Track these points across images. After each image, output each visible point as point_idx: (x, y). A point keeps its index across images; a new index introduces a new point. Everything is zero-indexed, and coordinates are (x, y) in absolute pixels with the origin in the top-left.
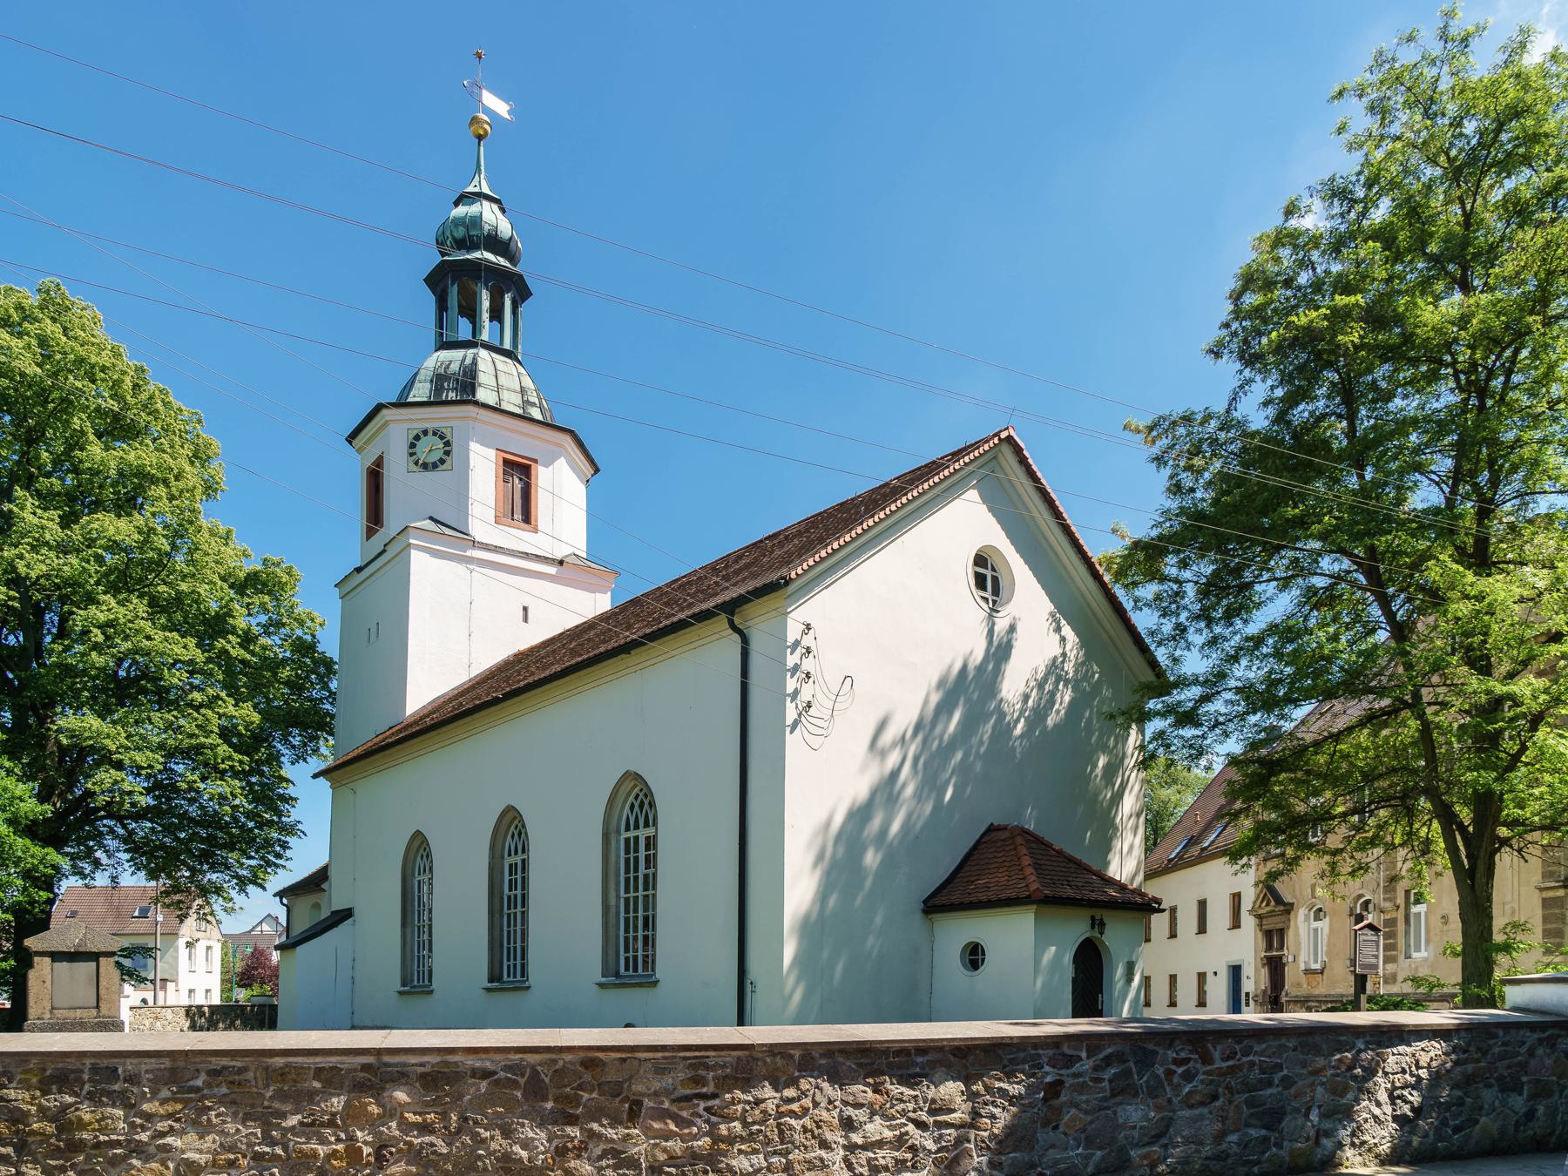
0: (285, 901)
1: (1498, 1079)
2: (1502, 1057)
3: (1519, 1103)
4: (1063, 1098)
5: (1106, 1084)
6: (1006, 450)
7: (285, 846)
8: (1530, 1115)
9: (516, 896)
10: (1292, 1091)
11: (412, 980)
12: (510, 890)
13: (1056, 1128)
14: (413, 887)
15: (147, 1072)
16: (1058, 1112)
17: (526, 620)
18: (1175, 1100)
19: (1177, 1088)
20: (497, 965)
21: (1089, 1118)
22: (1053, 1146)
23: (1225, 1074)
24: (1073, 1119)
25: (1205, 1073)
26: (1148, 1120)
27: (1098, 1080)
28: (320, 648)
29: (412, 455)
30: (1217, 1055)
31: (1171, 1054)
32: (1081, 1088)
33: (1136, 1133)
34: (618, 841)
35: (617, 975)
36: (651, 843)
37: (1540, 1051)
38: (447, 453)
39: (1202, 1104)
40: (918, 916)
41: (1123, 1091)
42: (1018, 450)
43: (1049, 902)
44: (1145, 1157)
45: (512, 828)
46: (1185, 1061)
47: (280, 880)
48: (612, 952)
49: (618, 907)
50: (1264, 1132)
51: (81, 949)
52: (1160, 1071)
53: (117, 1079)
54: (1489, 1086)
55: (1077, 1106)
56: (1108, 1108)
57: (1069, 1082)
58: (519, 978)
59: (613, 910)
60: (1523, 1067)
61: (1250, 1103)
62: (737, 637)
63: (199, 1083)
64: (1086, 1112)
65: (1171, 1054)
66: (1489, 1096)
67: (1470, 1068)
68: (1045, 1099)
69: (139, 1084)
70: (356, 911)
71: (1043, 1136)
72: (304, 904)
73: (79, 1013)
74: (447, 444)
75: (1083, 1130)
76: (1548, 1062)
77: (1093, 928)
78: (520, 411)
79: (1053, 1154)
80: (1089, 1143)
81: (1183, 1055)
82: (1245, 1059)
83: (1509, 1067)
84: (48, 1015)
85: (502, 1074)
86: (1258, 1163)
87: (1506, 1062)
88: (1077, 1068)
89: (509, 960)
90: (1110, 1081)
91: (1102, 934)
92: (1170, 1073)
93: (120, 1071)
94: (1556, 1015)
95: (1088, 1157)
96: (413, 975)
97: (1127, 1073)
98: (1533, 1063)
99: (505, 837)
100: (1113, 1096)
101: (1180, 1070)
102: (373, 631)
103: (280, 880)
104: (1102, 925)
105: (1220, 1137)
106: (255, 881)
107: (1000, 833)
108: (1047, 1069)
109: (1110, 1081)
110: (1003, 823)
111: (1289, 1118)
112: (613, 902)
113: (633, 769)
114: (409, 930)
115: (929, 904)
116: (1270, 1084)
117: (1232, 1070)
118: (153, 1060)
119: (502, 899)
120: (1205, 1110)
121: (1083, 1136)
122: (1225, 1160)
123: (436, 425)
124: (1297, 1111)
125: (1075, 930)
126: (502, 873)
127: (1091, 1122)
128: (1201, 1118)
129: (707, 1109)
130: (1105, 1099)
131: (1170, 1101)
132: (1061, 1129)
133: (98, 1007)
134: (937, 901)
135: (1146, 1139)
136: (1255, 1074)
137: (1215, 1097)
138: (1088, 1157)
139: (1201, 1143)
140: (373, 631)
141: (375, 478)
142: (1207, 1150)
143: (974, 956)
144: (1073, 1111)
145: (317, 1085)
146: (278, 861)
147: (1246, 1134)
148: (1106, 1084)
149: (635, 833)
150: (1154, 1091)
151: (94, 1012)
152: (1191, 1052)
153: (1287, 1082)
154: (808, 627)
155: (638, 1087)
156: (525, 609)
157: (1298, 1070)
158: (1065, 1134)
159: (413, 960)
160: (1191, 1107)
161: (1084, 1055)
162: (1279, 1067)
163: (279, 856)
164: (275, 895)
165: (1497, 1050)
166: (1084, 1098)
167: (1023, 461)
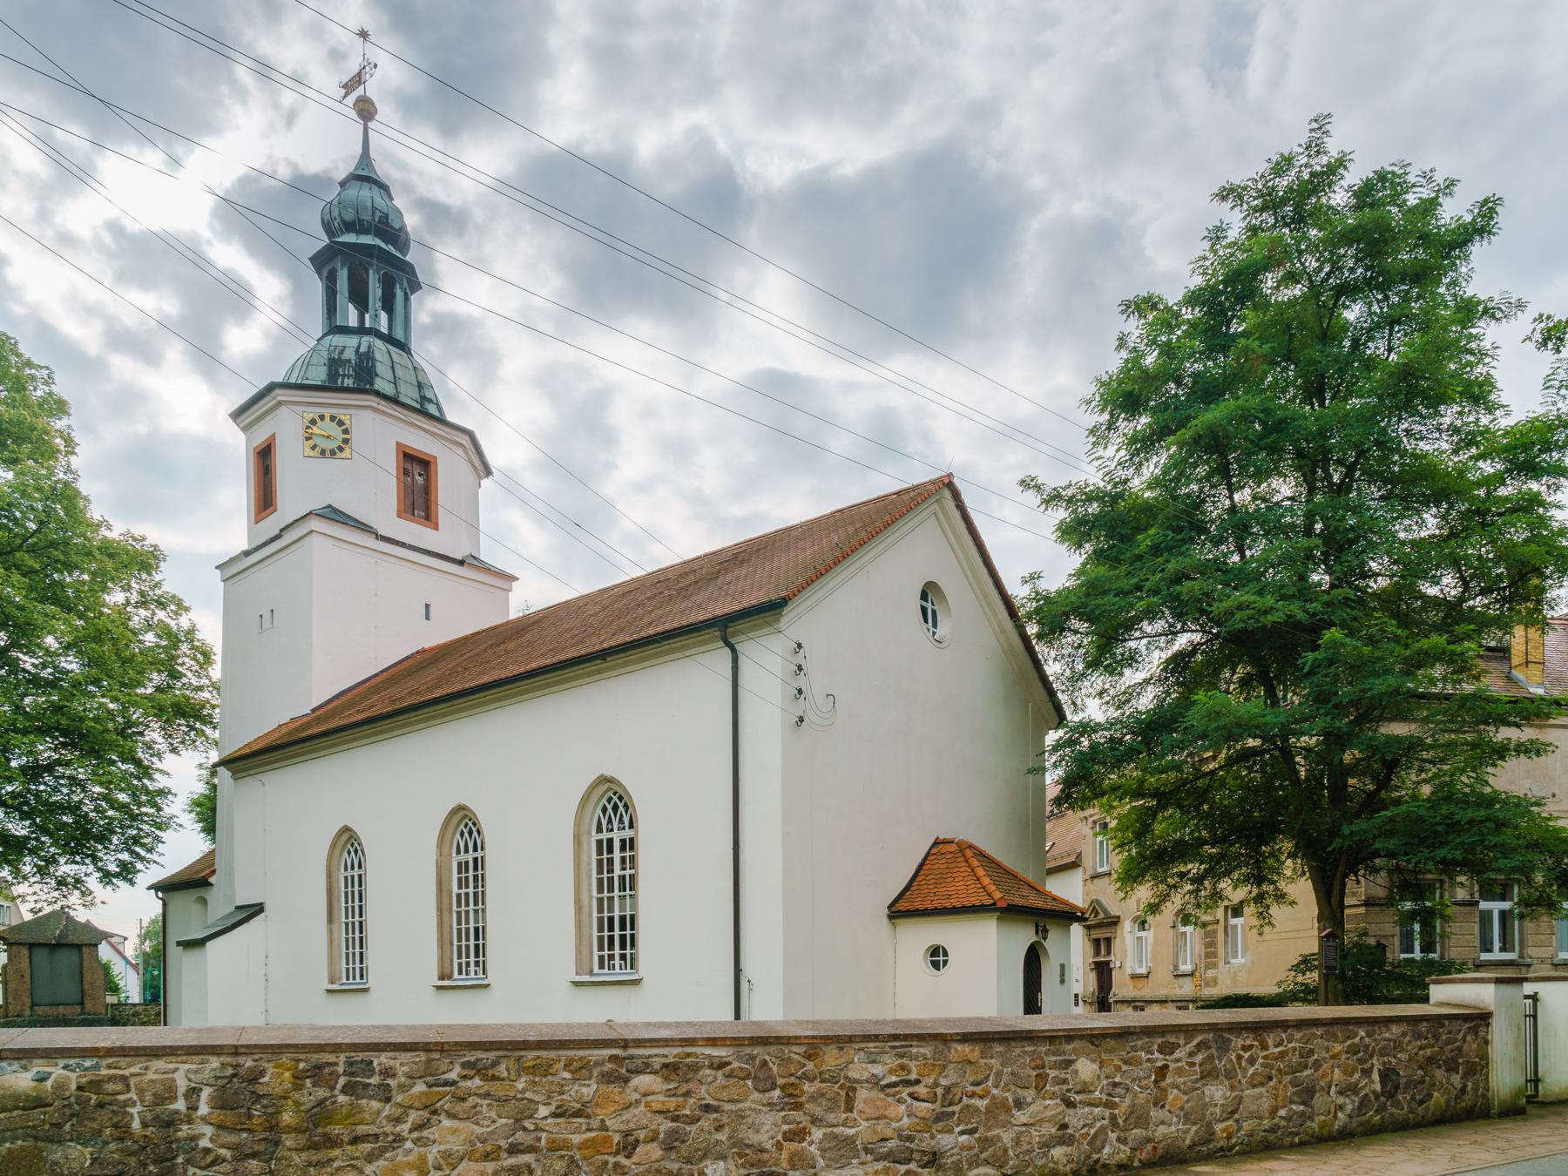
0: (160, 895)
1: (1445, 1062)
2: (1448, 1042)
3: (1456, 1079)
4: (1168, 1081)
5: (1197, 1067)
6: (947, 494)
7: (158, 839)
8: (1463, 1090)
9: (467, 895)
10: (1320, 1072)
11: (340, 978)
12: (460, 887)
13: (1163, 1106)
14: (338, 882)
15: (401, 1064)
16: (1164, 1090)
17: (427, 618)
18: (1243, 1081)
19: (1244, 1070)
20: (447, 964)
21: (1186, 1098)
22: (1162, 1123)
23: (1276, 1059)
24: (1175, 1099)
25: (1265, 1057)
26: (1226, 1098)
27: (1192, 1064)
28: (199, 636)
29: (308, 439)
30: (1270, 1042)
31: (1240, 1042)
32: (1180, 1072)
33: (1218, 1110)
34: (589, 843)
35: (591, 973)
36: (629, 845)
37: (1469, 1038)
38: (346, 441)
39: (1262, 1084)
40: (885, 920)
41: (1210, 1073)
42: (956, 496)
43: (1011, 912)
44: (1224, 1130)
45: (462, 827)
46: (1251, 1047)
47: (150, 875)
48: (585, 951)
49: (590, 906)
50: (1302, 1108)
51: (62, 941)
52: (1233, 1057)
53: (372, 1073)
54: (1439, 1067)
55: (1178, 1087)
56: (1198, 1089)
57: (1172, 1066)
58: (472, 975)
59: (585, 910)
60: (1460, 1049)
61: (1294, 1083)
62: (727, 650)
63: (453, 1075)
64: (1185, 1093)
65: (1240, 1042)
66: (1440, 1074)
67: (1429, 1052)
68: (1156, 1082)
69: (394, 1076)
70: (267, 907)
71: (1156, 1114)
72: (184, 902)
73: (61, 1009)
74: (346, 431)
75: (1182, 1109)
76: (1474, 1046)
77: (1037, 933)
78: (418, 406)
79: (1162, 1129)
80: (1187, 1118)
81: (1248, 1042)
82: (1290, 1046)
83: (1452, 1051)
84: (28, 1012)
85: (736, 1065)
86: (1298, 1134)
87: (1449, 1047)
88: (1177, 1054)
89: (460, 957)
90: (1200, 1065)
91: (1045, 939)
92: (1239, 1058)
93: (375, 1064)
94: (1475, 1008)
95: (1186, 1132)
96: (340, 972)
97: (1210, 1058)
98: (1465, 1047)
99: (454, 833)
100: (1202, 1078)
101: (1247, 1055)
102: (267, 617)
103: (150, 875)
104: (1045, 931)
105: (1273, 1112)
106: (127, 872)
107: (947, 846)
108: (1157, 1055)
109: (1200, 1065)
110: (949, 836)
111: (1317, 1095)
112: (585, 901)
113: (608, 773)
114: (335, 926)
115: (893, 909)
116: (1306, 1067)
117: (1282, 1055)
118: (409, 1054)
119: (451, 896)
120: (1263, 1090)
121: (1182, 1114)
122: (1276, 1132)
123: (334, 411)
124: (1322, 1088)
125: (1024, 936)
126: (450, 870)
127: (1188, 1101)
128: (1261, 1096)
129: (911, 1095)
130: (1196, 1081)
131: (1240, 1082)
132: (1167, 1107)
133: (82, 1003)
134: (901, 906)
135: (1225, 1115)
136: (1295, 1059)
137: (1270, 1078)
138: (1186, 1132)
139: (1261, 1118)
140: (267, 617)
141: (264, 456)
142: (1266, 1123)
143: (937, 957)
144: (1175, 1091)
145: (567, 1075)
146: (148, 856)
147: (1291, 1109)
148: (1197, 1067)
149: (610, 835)
150: (1230, 1075)
151: (78, 1009)
152: (1254, 1039)
153: (1317, 1065)
154: (800, 646)
155: (854, 1074)
156: (427, 606)
157: (1324, 1054)
158: (1170, 1111)
159: (340, 956)
160: (1254, 1086)
161: (1182, 1042)
162: (1312, 1052)
163: (150, 851)
164: (149, 888)
165: (1444, 1037)
166: (1182, 1080)
167: (961, 507)
